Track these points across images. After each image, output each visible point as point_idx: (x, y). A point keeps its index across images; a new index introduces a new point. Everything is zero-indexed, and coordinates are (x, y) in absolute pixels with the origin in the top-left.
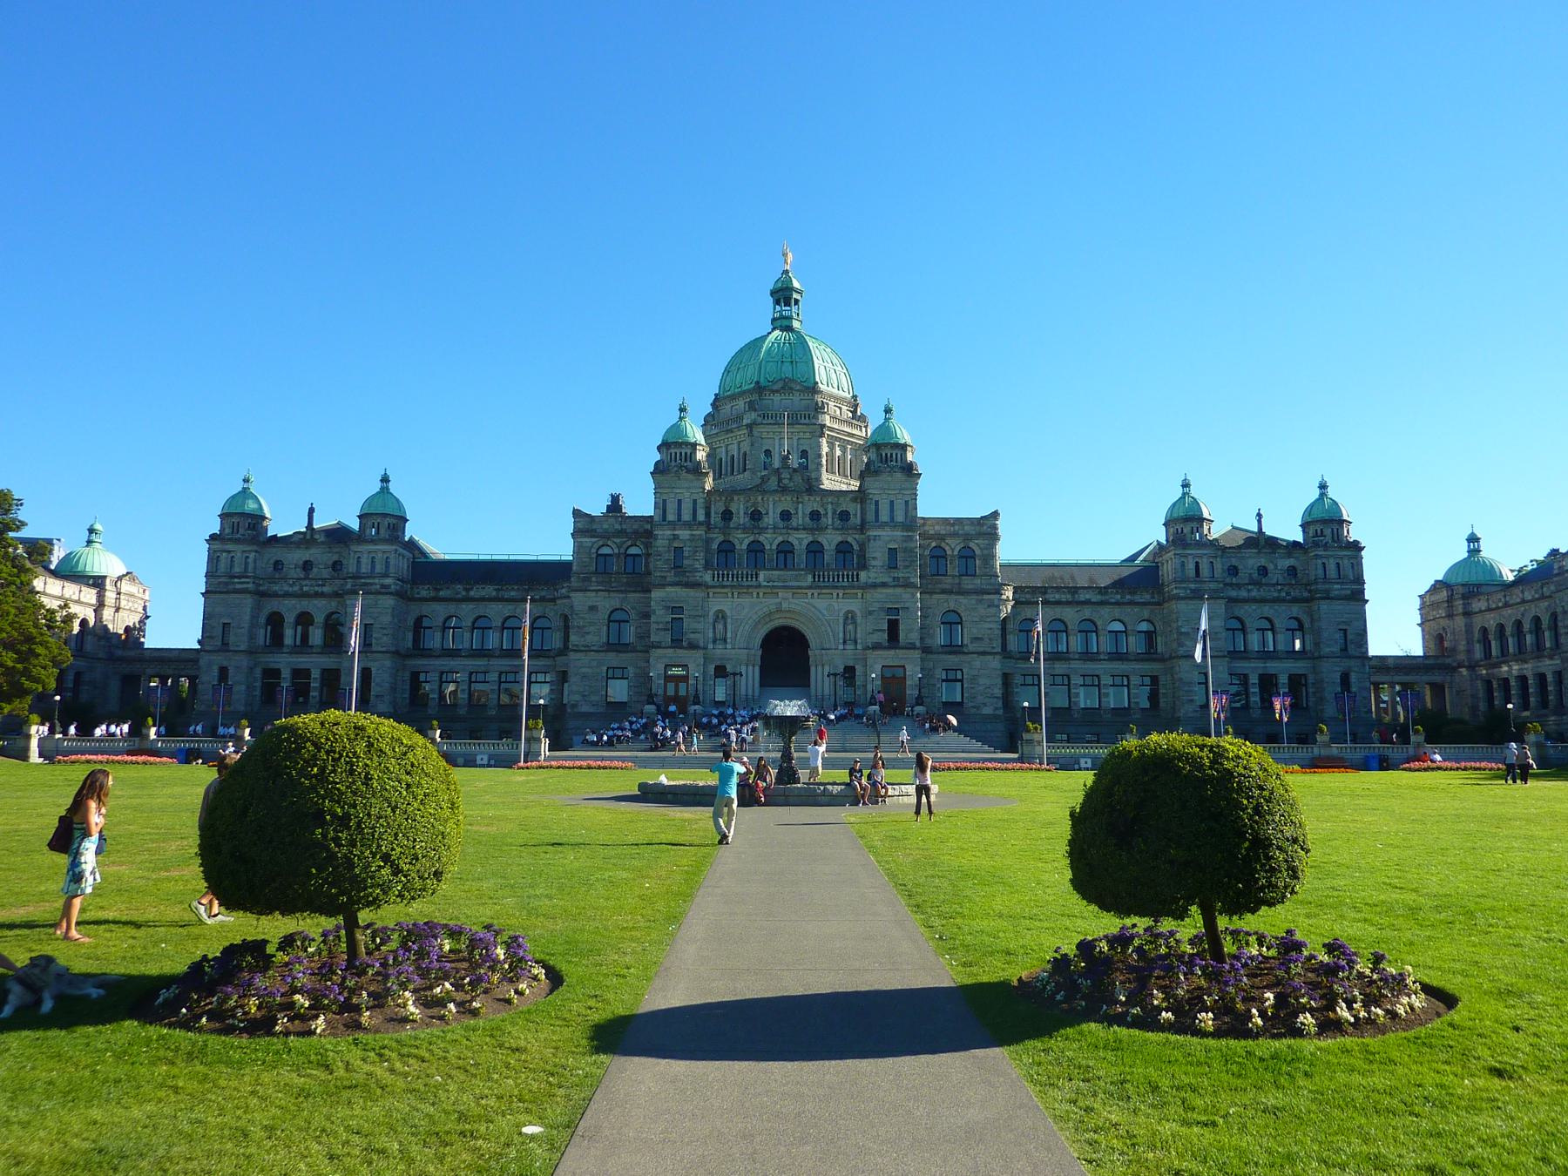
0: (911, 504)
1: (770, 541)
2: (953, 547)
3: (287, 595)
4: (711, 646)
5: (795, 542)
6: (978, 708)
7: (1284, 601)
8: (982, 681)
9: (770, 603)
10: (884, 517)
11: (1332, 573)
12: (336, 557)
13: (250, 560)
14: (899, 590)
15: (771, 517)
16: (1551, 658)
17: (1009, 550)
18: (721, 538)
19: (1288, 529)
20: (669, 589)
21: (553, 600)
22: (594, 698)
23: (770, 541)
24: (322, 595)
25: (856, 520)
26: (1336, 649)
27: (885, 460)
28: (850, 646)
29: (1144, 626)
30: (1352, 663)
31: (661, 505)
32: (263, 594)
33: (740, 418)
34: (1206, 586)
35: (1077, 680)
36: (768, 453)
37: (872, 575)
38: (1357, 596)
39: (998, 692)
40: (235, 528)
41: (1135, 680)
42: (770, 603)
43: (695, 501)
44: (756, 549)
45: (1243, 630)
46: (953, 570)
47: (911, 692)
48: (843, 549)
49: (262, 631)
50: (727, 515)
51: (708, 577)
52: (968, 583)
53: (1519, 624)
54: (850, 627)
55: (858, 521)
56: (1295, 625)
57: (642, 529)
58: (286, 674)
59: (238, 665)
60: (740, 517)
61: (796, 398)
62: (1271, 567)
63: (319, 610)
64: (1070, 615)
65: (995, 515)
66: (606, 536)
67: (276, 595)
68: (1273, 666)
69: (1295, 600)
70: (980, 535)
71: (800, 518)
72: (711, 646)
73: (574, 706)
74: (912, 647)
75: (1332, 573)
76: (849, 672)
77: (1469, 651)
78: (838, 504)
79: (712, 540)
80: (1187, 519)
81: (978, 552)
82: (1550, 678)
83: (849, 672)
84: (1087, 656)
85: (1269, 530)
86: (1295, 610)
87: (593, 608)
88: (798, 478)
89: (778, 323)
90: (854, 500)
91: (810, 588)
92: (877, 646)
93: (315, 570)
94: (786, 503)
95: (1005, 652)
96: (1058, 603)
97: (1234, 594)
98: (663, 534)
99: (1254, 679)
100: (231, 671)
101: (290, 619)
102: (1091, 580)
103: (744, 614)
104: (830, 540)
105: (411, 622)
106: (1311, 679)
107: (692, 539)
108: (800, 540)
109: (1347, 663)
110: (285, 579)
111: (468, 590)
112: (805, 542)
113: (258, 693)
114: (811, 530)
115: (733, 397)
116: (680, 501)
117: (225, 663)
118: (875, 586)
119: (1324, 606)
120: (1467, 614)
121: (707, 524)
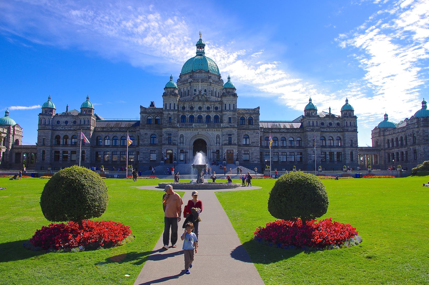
0: (235, 105)
1: (196, 115)
2: (247, 117)
3: (61, 130)
5: (203, 116)
6: (253, 161)
7: (336, 132)
8: (255, 154)
9: (196, 132)
10: (228, 108)
11: (349, 124)
12: (74, 120)
13: (51, 121)
15: (196, 109)
16: (405, 147)
17: (262, 118)
18: (182, 114)
19: (337, 113)
20: (167, 128)
21: (135, 132)
23: (196, 115)
24: (71, 130)
25: (219, 109)
26: (349, 145)
27: (228, 93)
29: (299, 139)
30: (354, 149)
31: (165, 105)
32: (54, 130)
33: (187, 80)
34: (315, 128)
35: (280, 153)
36: (195, 90)
37: (224, 124)
38: (356, 131)
39: (259, 157)
40: (46, 112)
41: (296, 154)
42: (196, 132)
44: (192, 117)
45: (325, 140)
47: (235, 157)
48: (216, 117)
49: (54, 140)
50: (184, 108)
51: (178, 125)
52: (251, 127)
53: (397, 138)
55: (220, 110)
56: (339, 138)
57: (160, 112)
58: (61, 152)
59: (48, 149)
60: (187, 109)
61: (203, 74)
62: (333, 123)
63: (70, 134)
64: (279, 136)
65: (259, 108)
66: (149, 113)
67: (58, 130)
68: (333, 150)
69: (339, 132)
70: (254, 113)
71: (204, 109)
73: (141, 161)
75: (349, 124)
76: (218, 151)
77: (384, 146)
78: (215, 105)
79: (180, 115)
80: (310, 110)
81: (254, 118)
82: (404, 153)
83: (218, 151)
84: (283, 147)
85: (332, 112)
86: (339, 134)
87: (146, 134)
89: (198, 54)
90: (219, 104)
91: (206, 128)
92: (225, 144)
93: (69, 123)
94: (200, 104)
96: (276, 132)
97: (323, 130)
98: (166, 113)
99: (328, 153)
100: (46, 151)
101: (62, 137)
102: (284, 126)
105: (95, 138)
106: (343, 153)
107: (174, 114)
108: (204, 115)
109: (352, 149)
111: (111, 129)
112: (206, 116)
113: (53, 157)
115: (185, 74)
116: (170, 104)
117: (44, 150)
118: (225, 128)
119: (346, 133)
120: (384, 135)
121: (178, 110)
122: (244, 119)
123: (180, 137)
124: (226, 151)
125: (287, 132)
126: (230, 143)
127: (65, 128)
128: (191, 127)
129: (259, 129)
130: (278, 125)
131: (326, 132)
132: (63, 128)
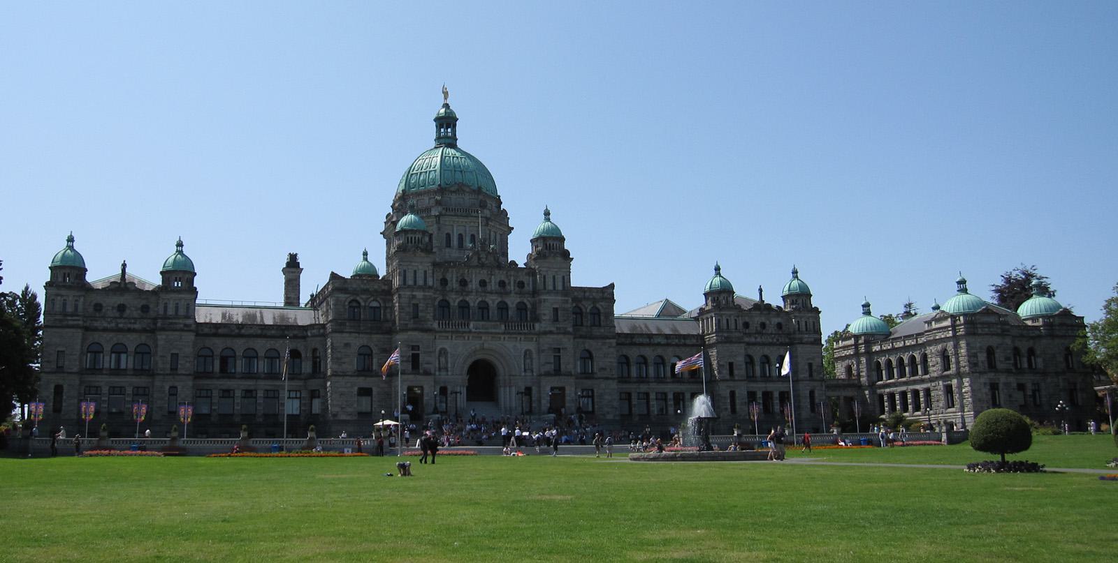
1: (474, 301)
3: (105, 330)
4: (437, 373)
5: (490, 302)
6: (604, 415)
12: (144, 302)
14: (561, 336)
15: (474, 285)
17: (619, 309)
18: (441, 298)
20: (410, 333)
22: (350, 410)
23: (474, 301)
24: (134, 331)
28: (529, 374)
30: (816, 384)
32: (87, 329)
35: (652, 396)
43: (425, 272)
46: (588, 321)
48: (521, 308)
50: (444, 282)
51: (435, 325)
52: (596, 331)
54: (528, 361)
60: (454, 283)
61: (467, 197)
62: (768, 322)
65: (612, 286)
67: (96, 329)
68: (771, 387)
70: (603, 299)
72: (437, 373)
73: (335, 415)
74: (569, 374)
76: (528, 391)
81: (602, 311)
83: (528, 391)
87: (347, 345)
88: (491, 259)
89: (443, 141)
90: (528, 274)
91: (504, 333)
92: (548, 374)
93: (128, 312)
94: (483, 274)
95: (623, 379)
96: (642, 344)
97: (747, 339)
99: (670, 396)
100: (65, 387)
101: (107, 348)
103: (458, 351)
104: (512, 301)
107: (425, 298)
108: (494, 301)
110: (104, 317)
112: (496, 302)
114: (500, 294)
115: (418, 194)
116: (415, 272)
117: (61, 382)
118: (545, 333)
122: (581, 314)
123: (439, 356)
124: (548, 388)
125: (668, 345)
126: (557, 372)
127: (117, 324)
128: (467, 330)
129: (614, 338)
130: (643, 327)
131: (754, 344)
132: (113, 325)
